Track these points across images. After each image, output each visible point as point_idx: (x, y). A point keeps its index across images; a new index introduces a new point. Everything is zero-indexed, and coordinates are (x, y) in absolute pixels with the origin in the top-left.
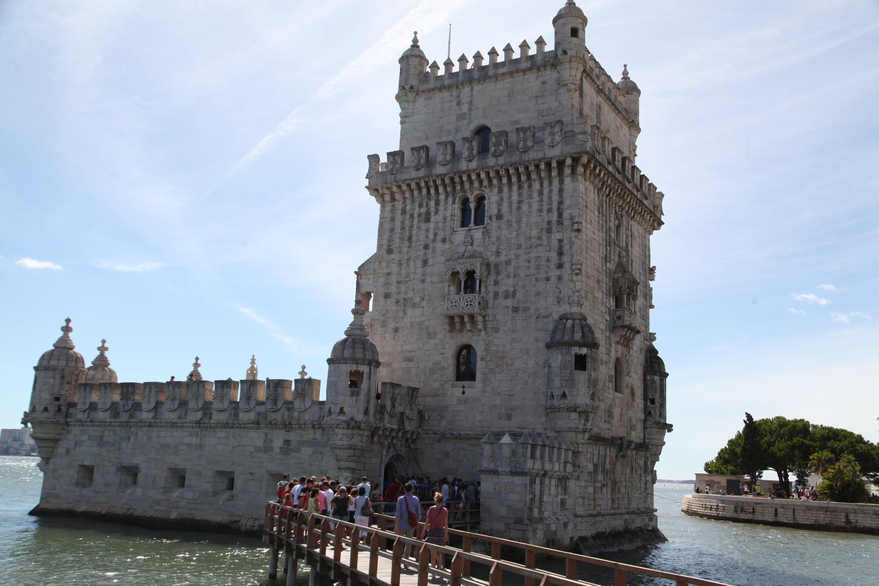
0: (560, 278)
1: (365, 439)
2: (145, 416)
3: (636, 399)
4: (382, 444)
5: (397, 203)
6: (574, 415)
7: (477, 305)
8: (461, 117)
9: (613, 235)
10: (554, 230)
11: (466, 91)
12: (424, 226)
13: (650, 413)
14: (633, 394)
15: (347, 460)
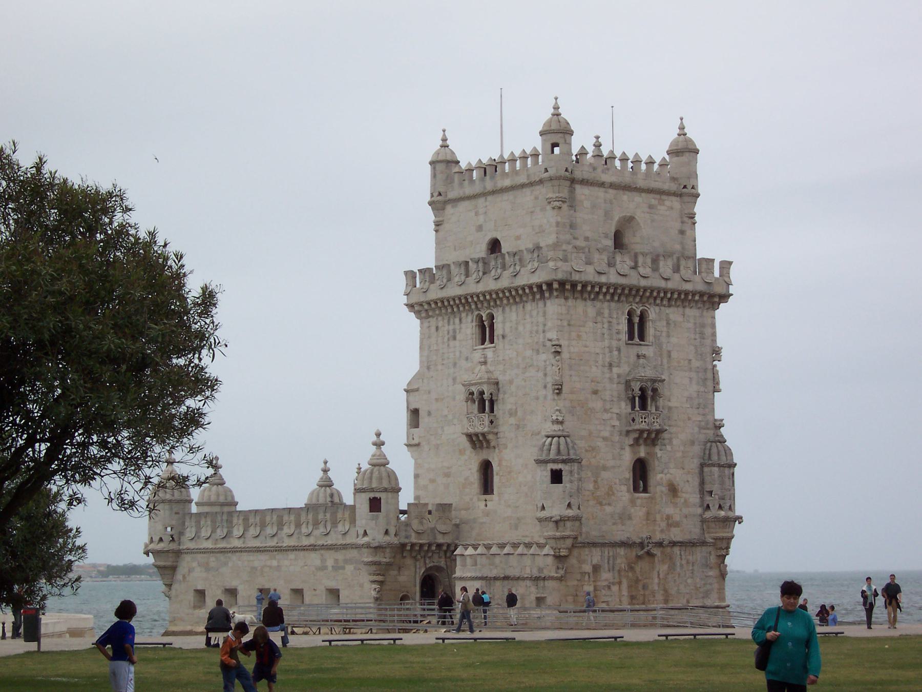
0: (545, 397)
1: (387, 555)
2: (237, 543)
3: (679, 494)
4: (415, 558)
5: (431, 319)
6: (551, 525)
7: (487, 422)
8: (480, 228)
9: (624, 337)
10: (541, 351)
11: (481, 201)
12: (452, 343)
13: (708, 507)
14: (673, 490)
15: (374, 575)
